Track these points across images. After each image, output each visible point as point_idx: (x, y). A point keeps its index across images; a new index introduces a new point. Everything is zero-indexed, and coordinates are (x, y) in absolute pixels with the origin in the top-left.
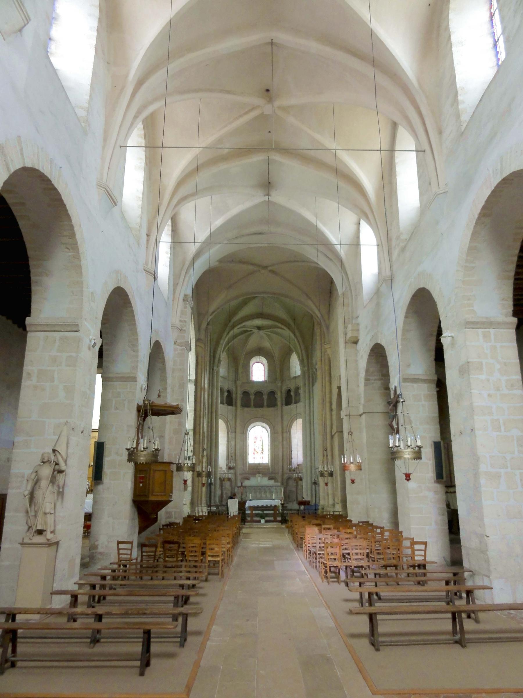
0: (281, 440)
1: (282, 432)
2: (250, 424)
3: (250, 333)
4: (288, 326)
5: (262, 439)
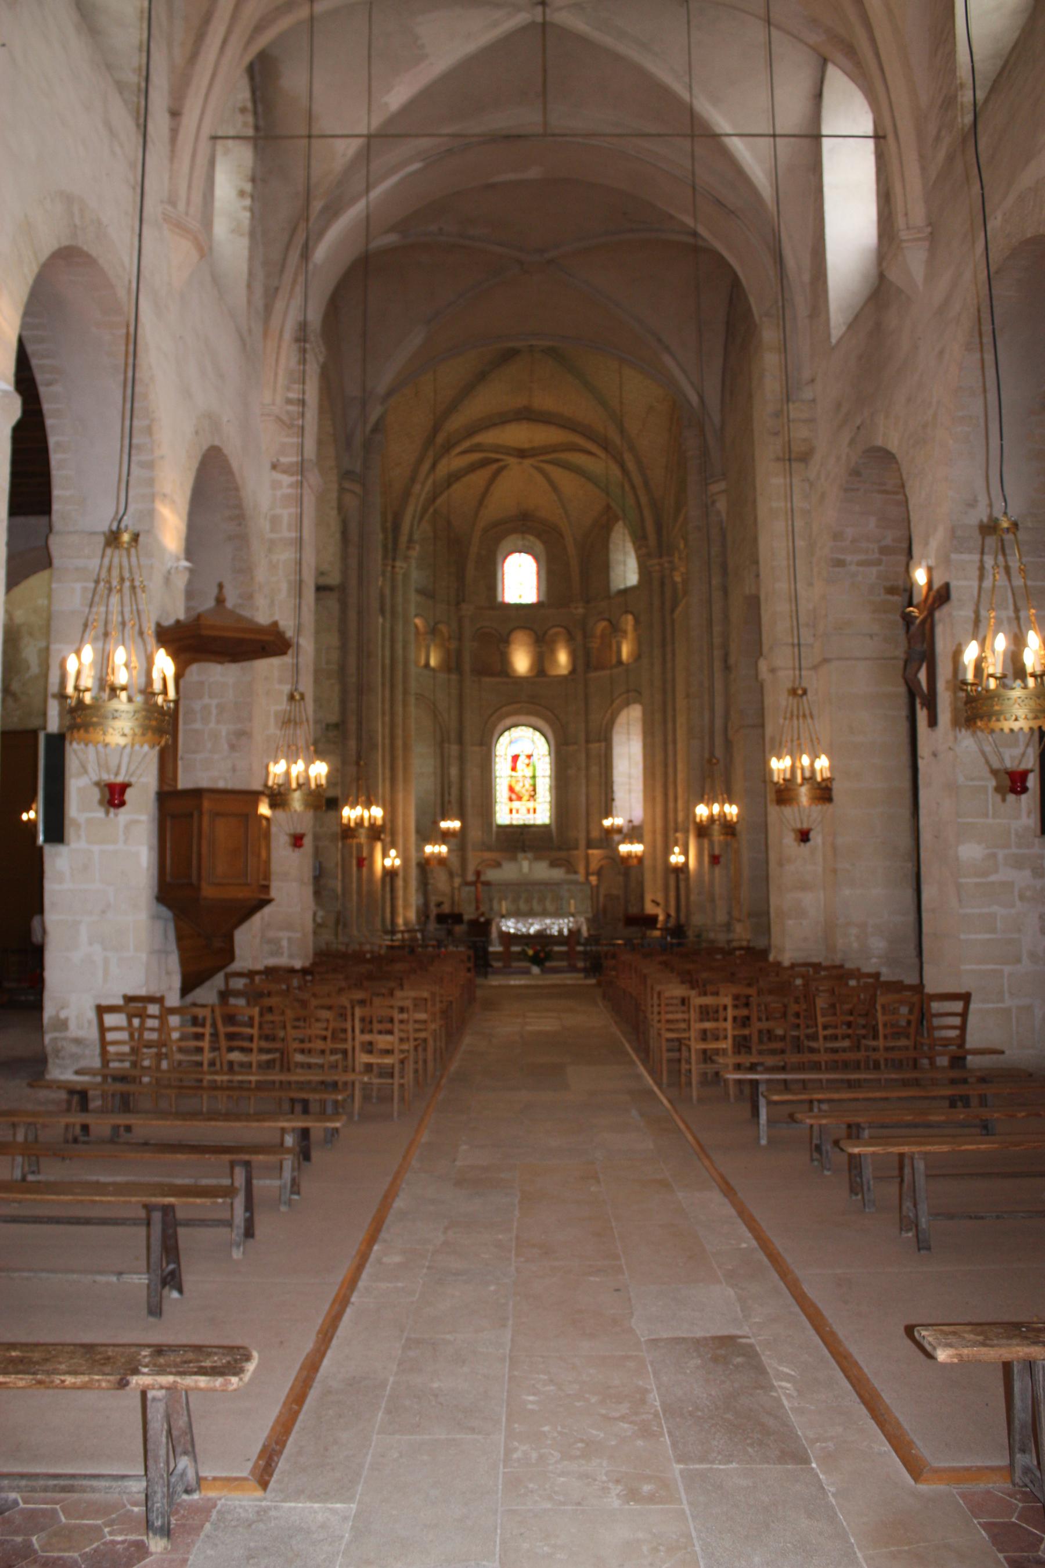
0: (583, 764)
2: (501, 718)
3: (495, 466)
4: (605, 445)
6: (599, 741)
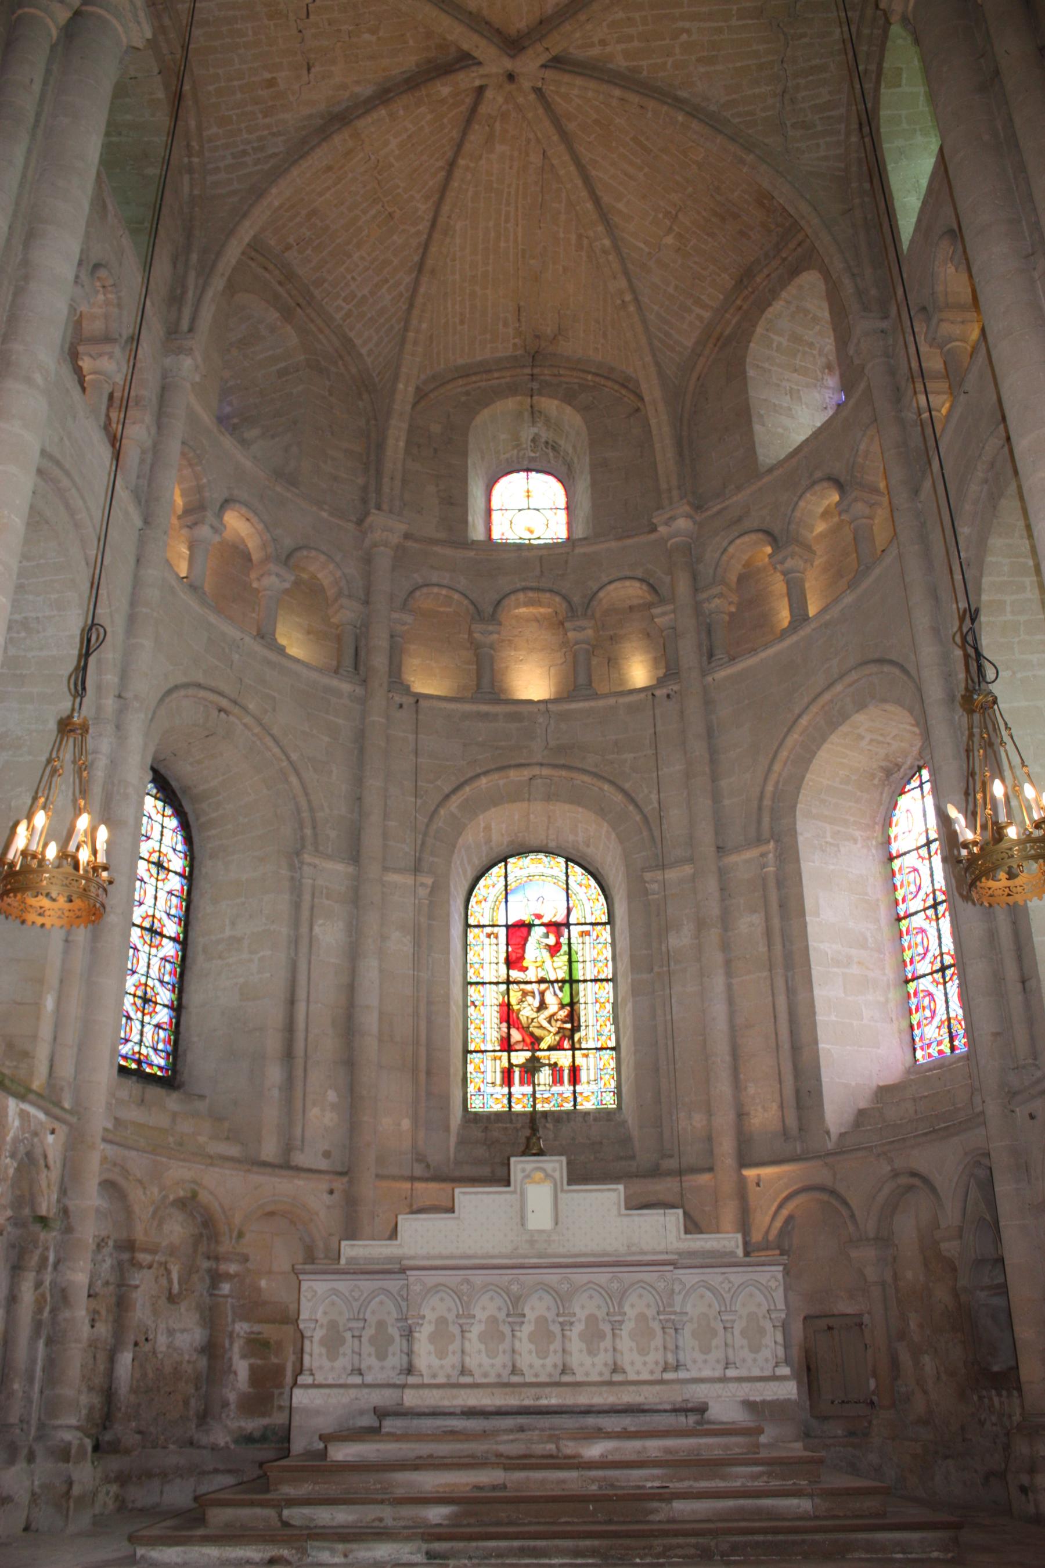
0: (713, 909)
1: (719, 848)
5: (564, 940)
6: (759, 841)
